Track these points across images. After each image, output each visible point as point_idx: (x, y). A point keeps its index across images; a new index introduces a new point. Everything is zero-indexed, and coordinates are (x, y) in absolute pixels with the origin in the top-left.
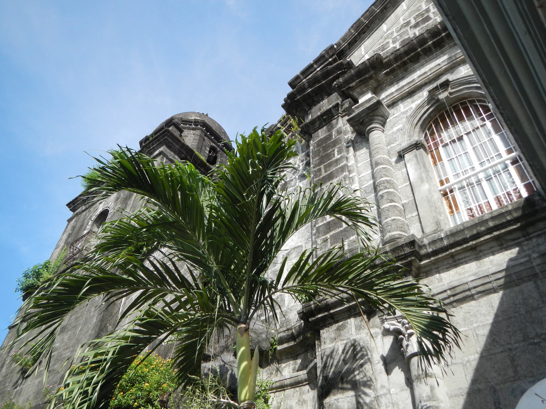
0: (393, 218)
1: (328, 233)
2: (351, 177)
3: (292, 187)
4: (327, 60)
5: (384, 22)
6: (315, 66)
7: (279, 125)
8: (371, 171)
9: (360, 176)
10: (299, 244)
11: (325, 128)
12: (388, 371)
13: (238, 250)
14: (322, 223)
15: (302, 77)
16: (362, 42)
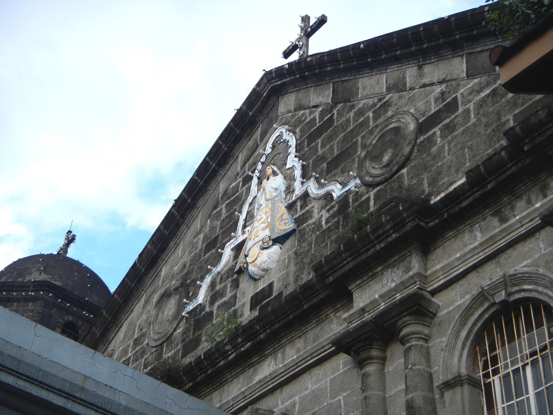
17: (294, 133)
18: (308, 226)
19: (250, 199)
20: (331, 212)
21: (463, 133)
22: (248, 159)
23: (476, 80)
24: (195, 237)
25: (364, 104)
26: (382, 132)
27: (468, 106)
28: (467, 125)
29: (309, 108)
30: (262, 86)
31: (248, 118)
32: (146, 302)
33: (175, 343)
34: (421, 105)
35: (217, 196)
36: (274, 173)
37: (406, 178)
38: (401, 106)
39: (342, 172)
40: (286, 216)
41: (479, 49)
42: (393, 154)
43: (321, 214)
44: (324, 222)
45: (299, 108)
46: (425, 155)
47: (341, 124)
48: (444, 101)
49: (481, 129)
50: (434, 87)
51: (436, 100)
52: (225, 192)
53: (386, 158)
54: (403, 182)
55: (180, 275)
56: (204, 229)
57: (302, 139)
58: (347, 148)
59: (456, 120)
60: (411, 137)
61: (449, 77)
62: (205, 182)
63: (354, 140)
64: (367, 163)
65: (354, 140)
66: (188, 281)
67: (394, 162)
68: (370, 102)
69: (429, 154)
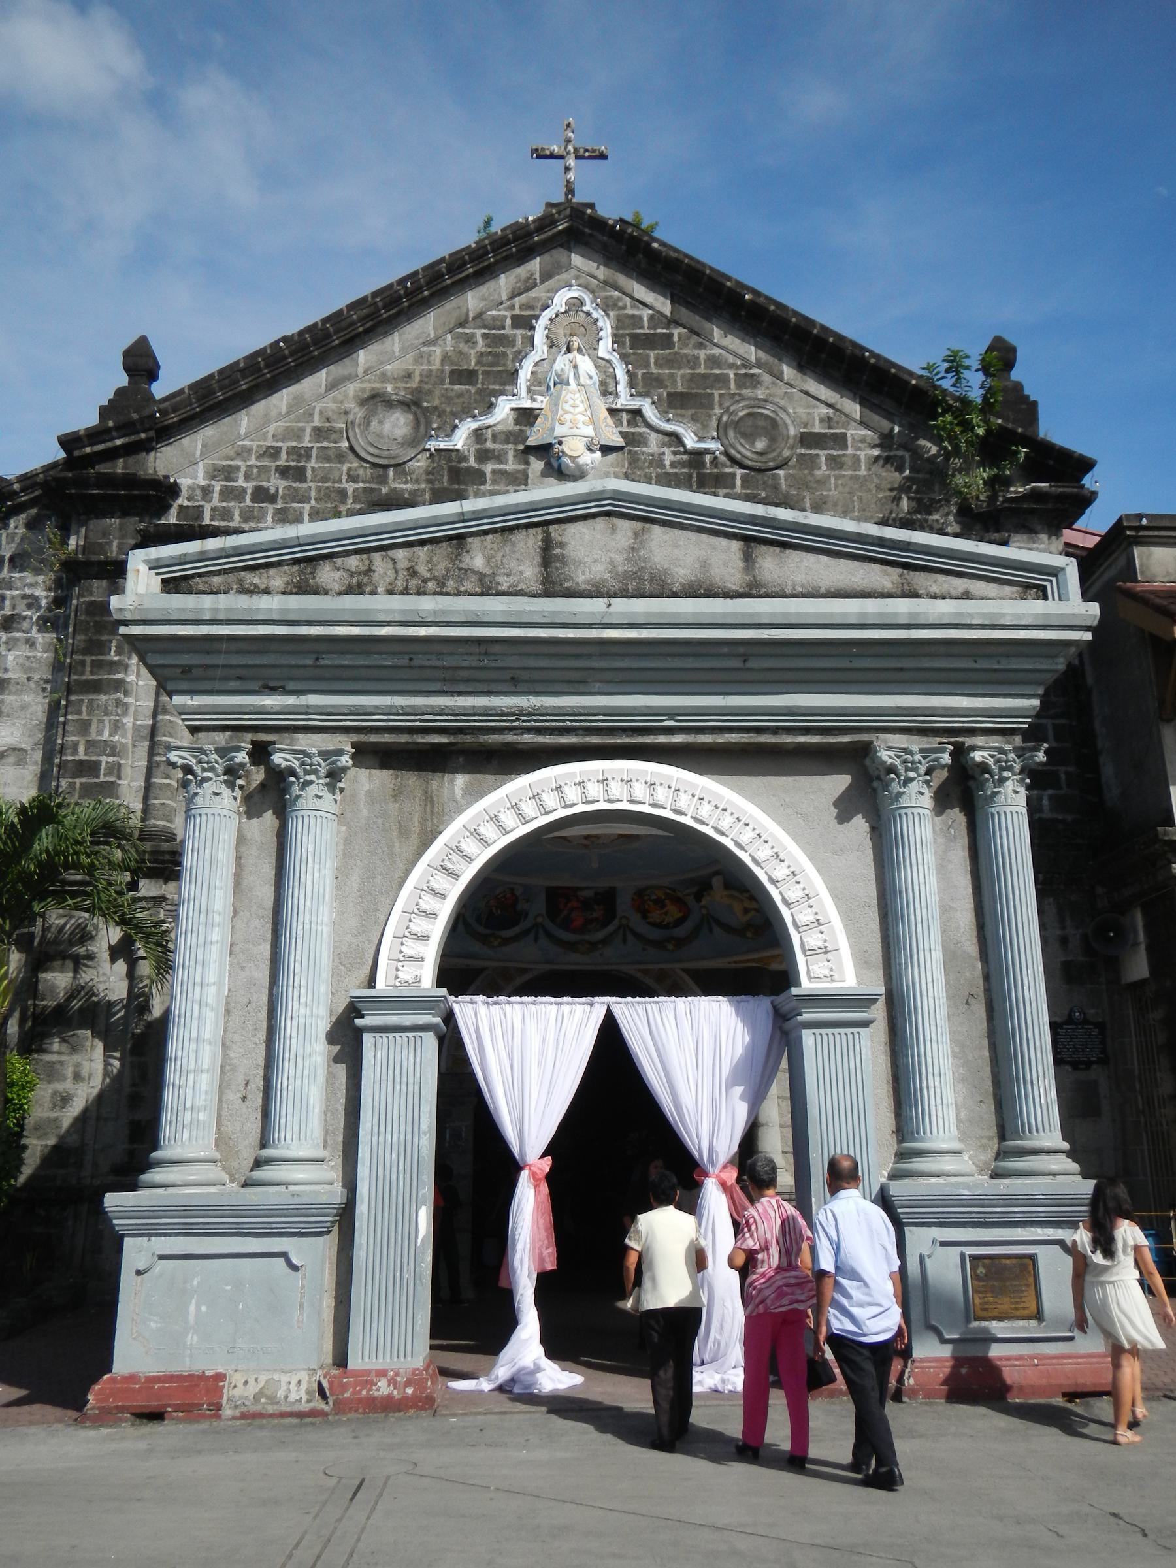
0: (162, 802)
1: (78, 777)
2: (126, 704)
3: (24, 632)
4: (138, 433)
5: (246, 407)
6: (114, 434)
7: (16, 487)
8: (153, 704)
9: (138, 703)
10: (23, 746)
11: (104, 583)
12: (113, 960)
13: (30, 901)
14: (72, 758)
15: (85, 440)
16: (202, 424)
17: (608, 315)
18: (643, 453)
19: (534, 357)
20: (678, 457)
21: (852, 477)
22: (520, 294)
23: (869, 432)
24: (424, 344)
25: (720, 354)
26: (751, 410)
27: (858, 453)
28: (857, 473)
29: (632, 298)
30: (562, 216)
31: (531, 242)
32: (333, 386)
33: (414, 477)
34: (801, 411)
35: (465, 310)
36: (579, 350)
37: (783, 481)
38: (775, 395)
39: (694, 419)
40: (610, 421)
41: (875, 402)
42: (769, 446)
43: (662, 450)
44: (667, 463)
45: (616, 287)
46: (806, 472)
47: (686, 356)
48: (830, 428)
49: (872, 487)
50: (818, 403)
51: (821, 421)
52: (479, 315)
53: (760, 445)
54: (779, 484)
55: (404, 385)
56: (440, 342)
57: (621, 332)
58: (697, 395)
59: (843, 459)
60: (791, 441)
61: (838, 407)
62: (453, 283)
63: (708, 391)
64: (731, 434)
65: (708, 391)
66: (425, 404)
67: (771, 456)
68: (731, 359)
69: (813, 475)
